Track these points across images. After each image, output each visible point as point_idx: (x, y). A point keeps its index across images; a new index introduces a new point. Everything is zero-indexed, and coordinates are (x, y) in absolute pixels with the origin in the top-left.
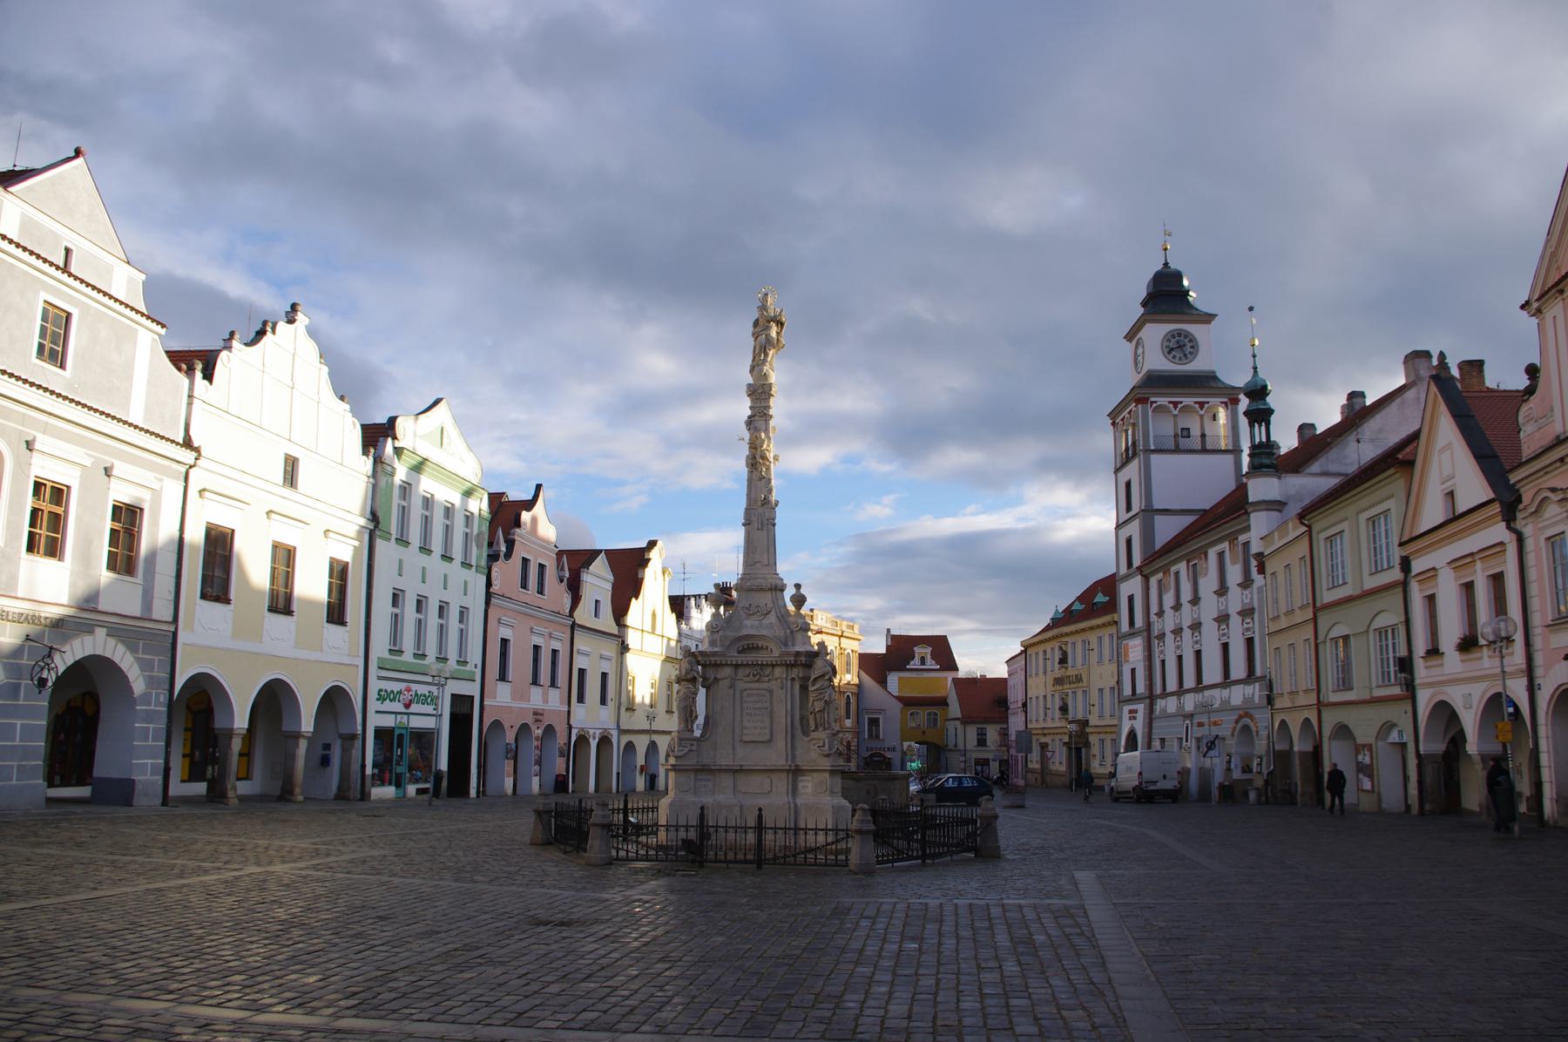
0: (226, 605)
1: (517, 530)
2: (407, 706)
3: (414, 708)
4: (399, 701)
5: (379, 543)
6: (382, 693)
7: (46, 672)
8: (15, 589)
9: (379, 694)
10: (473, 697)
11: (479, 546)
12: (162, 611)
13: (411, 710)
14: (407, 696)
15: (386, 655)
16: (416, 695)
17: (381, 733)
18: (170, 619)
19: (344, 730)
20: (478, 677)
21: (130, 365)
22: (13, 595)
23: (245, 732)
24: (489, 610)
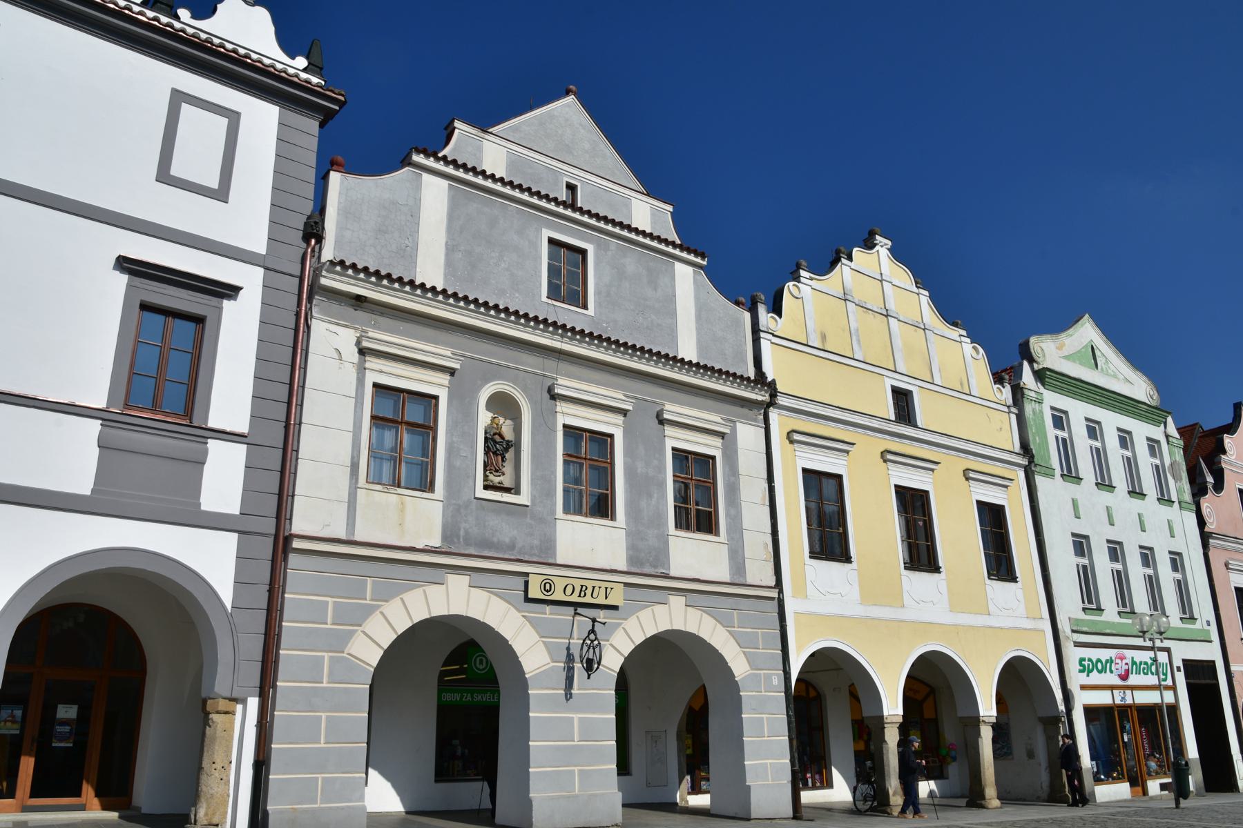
0: (850, 564)
1: (1223, 456)
2: (1124, 677)
3: (1134, 680)
4: (1111, 672)
5: (1040, 480)
6: (1086, 663)
7: (591, 650)
8: (554, 555)
9: (1081, 664)
10: (1213, 662)
11: (1177, 478)
12: (760, 573)
13: (1134, 680)
14: (1121, 667)
15: (1082, 616)
16: (1134, 663)
17: (1092, 713)
18: (773, 583)
19: (1045, 713)
20: (1215, 636)
21: (671, 299)
22: (551, 561)
23: (901, 720)
24: (1210, 554)
